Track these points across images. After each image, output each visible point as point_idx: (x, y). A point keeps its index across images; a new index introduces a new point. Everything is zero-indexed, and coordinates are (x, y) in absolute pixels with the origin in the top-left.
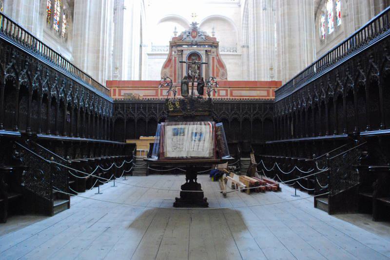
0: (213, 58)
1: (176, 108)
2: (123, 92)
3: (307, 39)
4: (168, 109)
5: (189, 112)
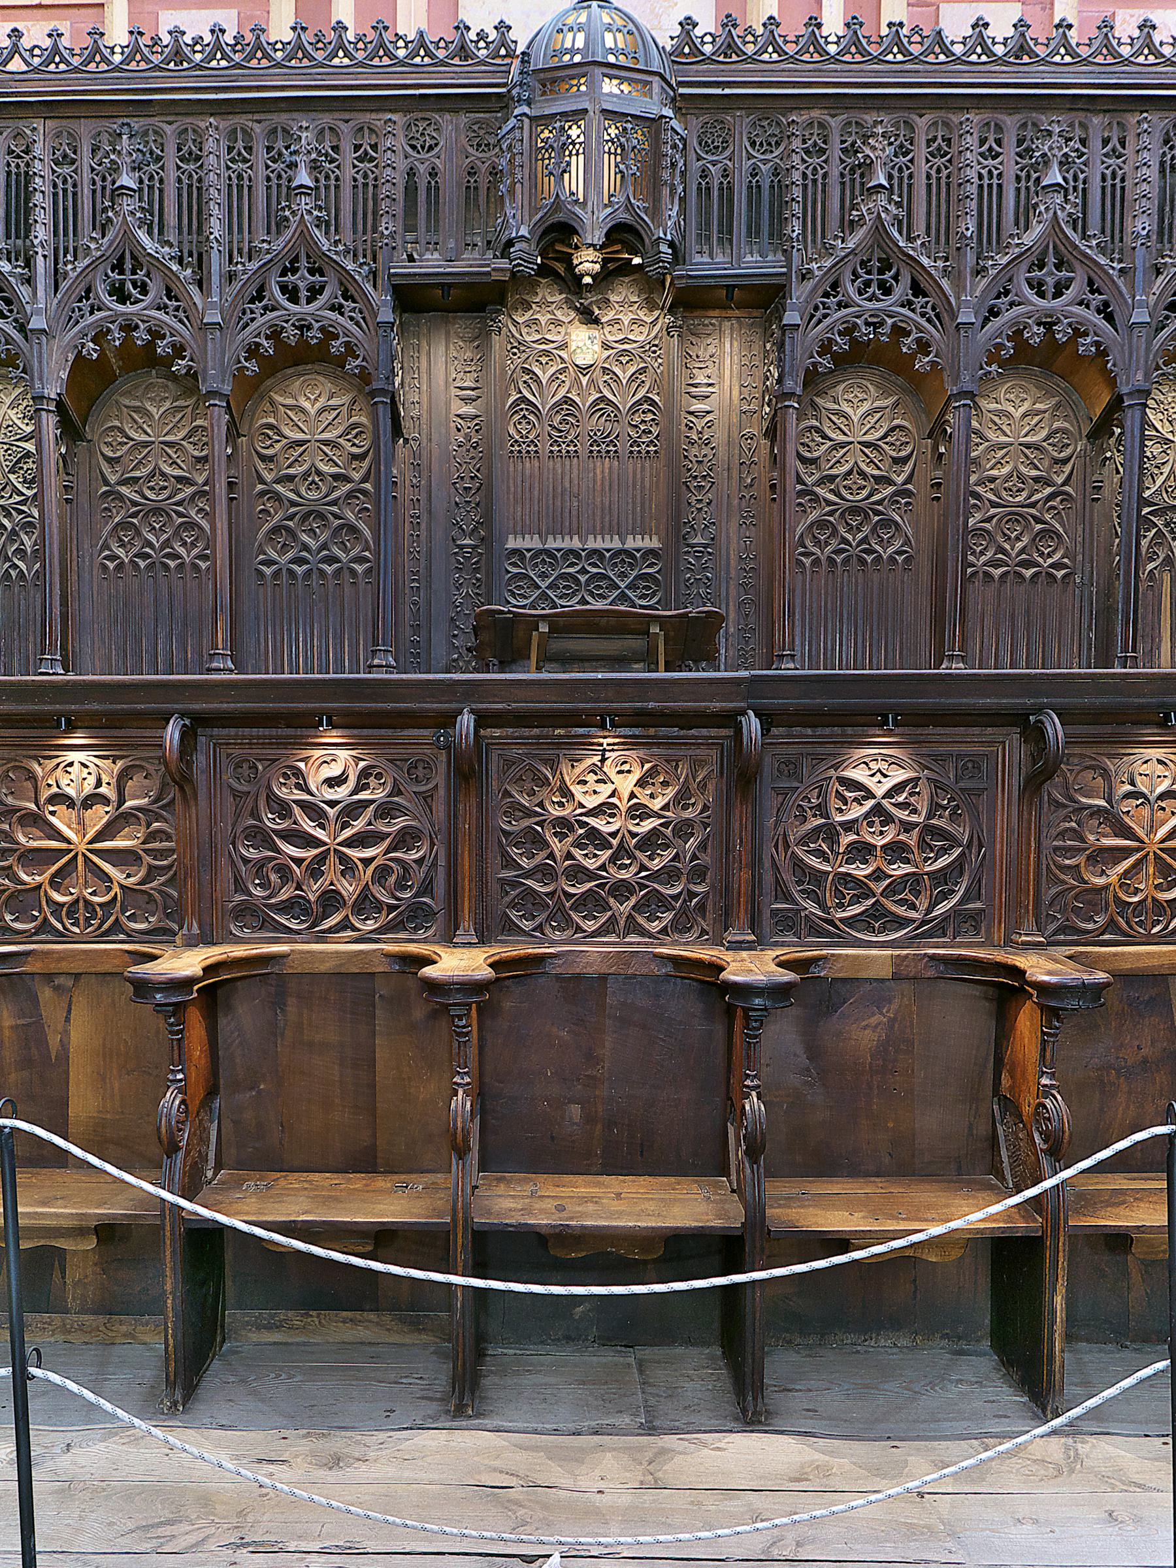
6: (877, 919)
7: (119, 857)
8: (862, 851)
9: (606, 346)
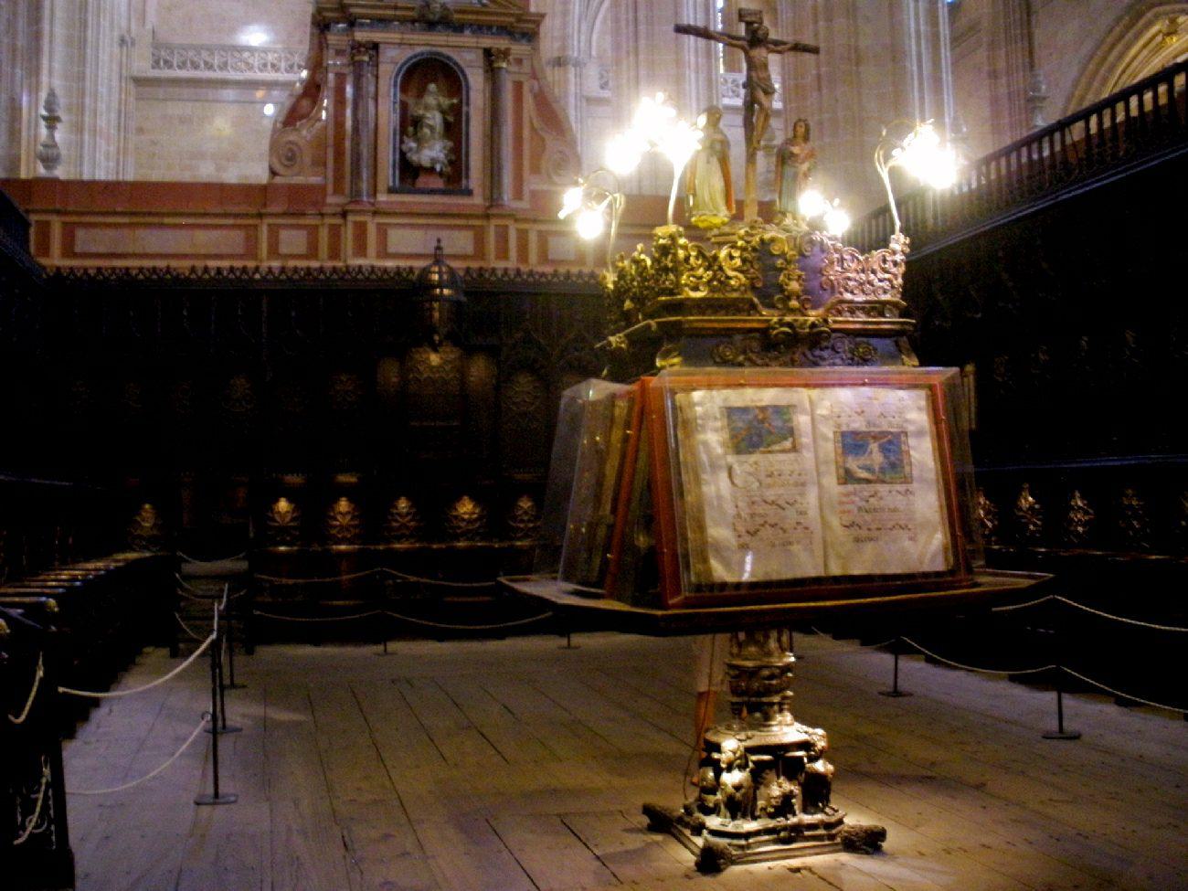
0: (518, 86)
1: (724, 283)
2: (83, 239)
3: (918, 32)
4: (677, 288)
5: (792, 311)
6: (526, 536)
7: (352, 526)
8: (522, 521)
9: (441, 358)
